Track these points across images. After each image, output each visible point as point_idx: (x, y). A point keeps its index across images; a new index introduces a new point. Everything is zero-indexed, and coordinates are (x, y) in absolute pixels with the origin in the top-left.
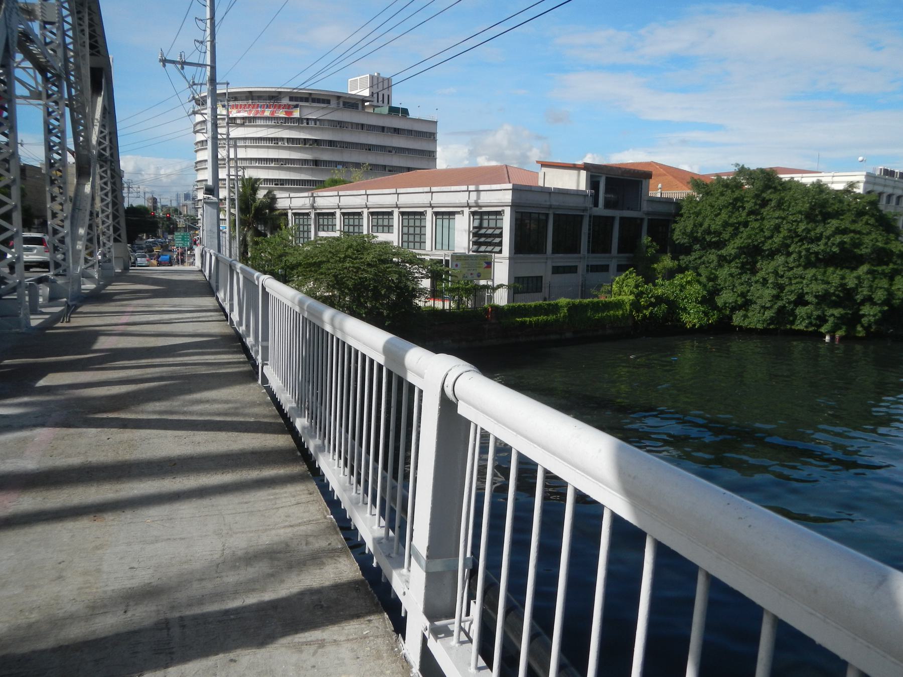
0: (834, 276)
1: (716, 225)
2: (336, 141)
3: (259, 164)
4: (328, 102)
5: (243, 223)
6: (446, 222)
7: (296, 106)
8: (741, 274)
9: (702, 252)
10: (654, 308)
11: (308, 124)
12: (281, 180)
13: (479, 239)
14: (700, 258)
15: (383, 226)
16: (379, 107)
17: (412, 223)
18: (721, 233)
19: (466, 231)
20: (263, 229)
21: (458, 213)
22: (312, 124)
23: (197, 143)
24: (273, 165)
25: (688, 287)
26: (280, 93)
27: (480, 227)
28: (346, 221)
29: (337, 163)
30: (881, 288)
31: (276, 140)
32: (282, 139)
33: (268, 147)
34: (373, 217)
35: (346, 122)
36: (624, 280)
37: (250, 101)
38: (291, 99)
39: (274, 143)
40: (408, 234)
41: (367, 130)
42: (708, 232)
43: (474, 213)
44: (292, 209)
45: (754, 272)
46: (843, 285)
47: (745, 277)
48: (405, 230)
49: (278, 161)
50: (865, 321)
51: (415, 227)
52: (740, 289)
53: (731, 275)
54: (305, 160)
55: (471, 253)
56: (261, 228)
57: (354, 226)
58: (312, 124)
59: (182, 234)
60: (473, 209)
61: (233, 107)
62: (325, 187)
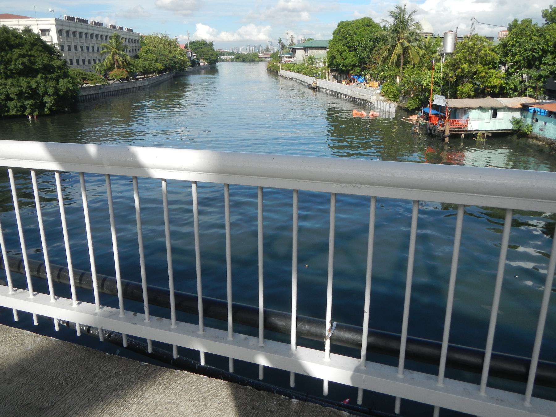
0: (23, 81)
30: (51, 86)
46: (30, 87)
50: (48, 105)
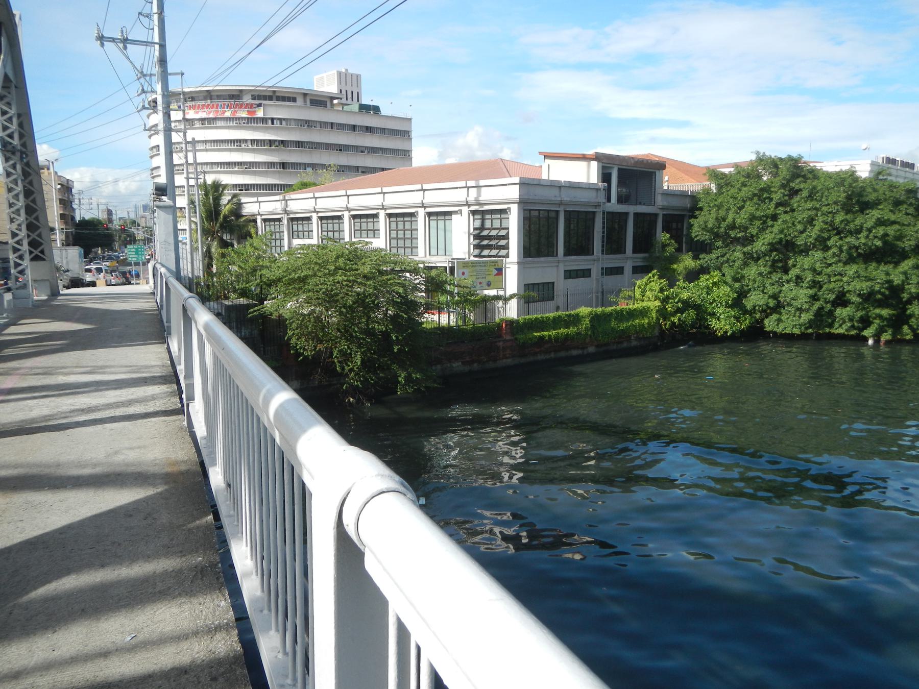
1: (742, 219)
2: (304, 142)
3: (221, 168)
4: (294, 100)
5: (206, 232)
6: (441, 223)
7: (259, 105)
8: (770, 273)
9: (725, 250)
10: (682, 314)
11: (273, 123)
12: (245, 185)
13: (481, 242)
14: (723, 256)
15: (368, 230)
16: (348, 105)
17: (401, 225)
18: (746, 228)
19: (465, 233)
20: (229, 238)
21: (456, 212)
22: (277, 123)
23: (152, 149)
24: (236, 169)
25: (715, 289)
26: (241, 91)
27: (482, 228)
28: (325, 226)
29: (306, 166)
31: (239, 141)
32: (246, 141)
33: (230, 150)
34: (356, 221)
35: (314, 121)
36: (646, 284)
37: (209, 101)
38: (254, 98)
39: (237, 146)
40: (397, 239)
41: (337, 129)
42: (733, 227)
43: (474, 213)
44: (261, 215)
45: (786, 271)
47: (775, 277)
48: (394, 234)
49: (241, 165)
51: (404, 230)
52: (771, 290)
53: (760, 274)
54: (271, 163)
55: (472, 258)
56: (226, 237)
57: (334, 231)
58: (277, 123)
59: (136, 247)
60: (473, 208)
61: (190, 108)
62: (294, 190)
